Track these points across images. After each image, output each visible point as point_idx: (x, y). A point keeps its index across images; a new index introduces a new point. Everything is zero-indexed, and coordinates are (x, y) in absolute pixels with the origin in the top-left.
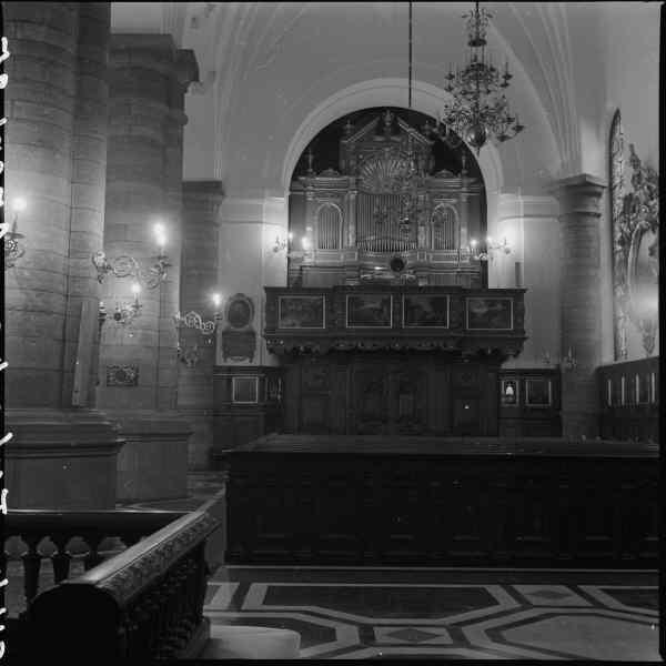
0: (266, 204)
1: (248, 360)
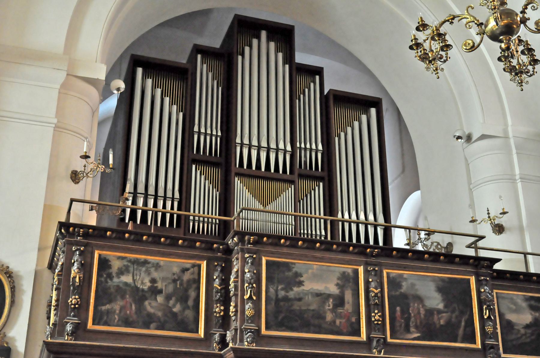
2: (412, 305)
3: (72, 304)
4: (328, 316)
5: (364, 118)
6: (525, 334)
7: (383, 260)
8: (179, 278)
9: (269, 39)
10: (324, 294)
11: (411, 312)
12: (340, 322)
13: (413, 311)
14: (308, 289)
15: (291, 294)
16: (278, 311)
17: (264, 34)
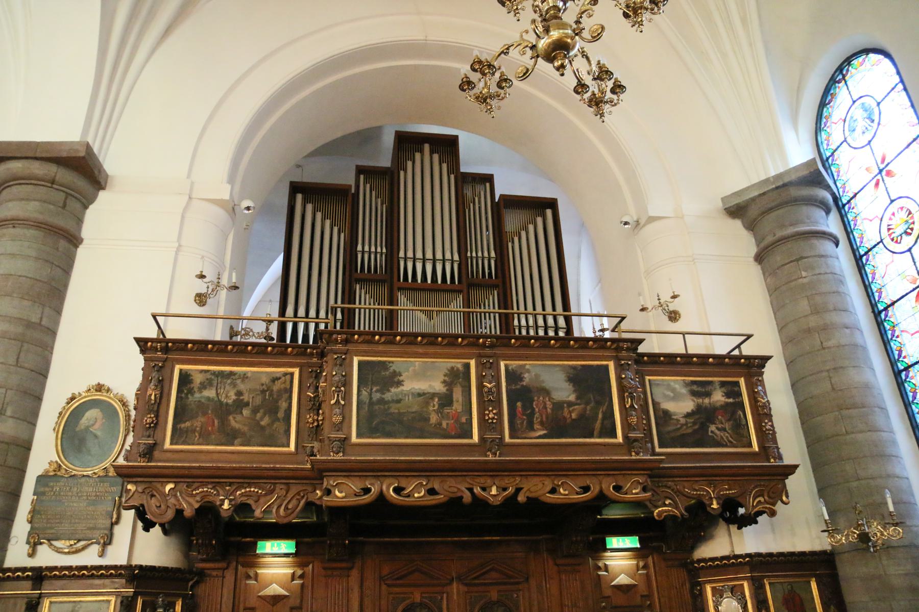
1: (95, 549)
2: (536, 398)
3: (147, 424)
4: (433, 418)
5: (539, 220)
6: (686, 424)
7: (498, 351)
8: (269, 389)
9: (432, 152)
10: (429, 393)
11: (535, 406)
12: (447, 424)
13: (537, 405)
14: (408, 389)
15: (388, 396)
16: (371, 415)
17: (427, 147)
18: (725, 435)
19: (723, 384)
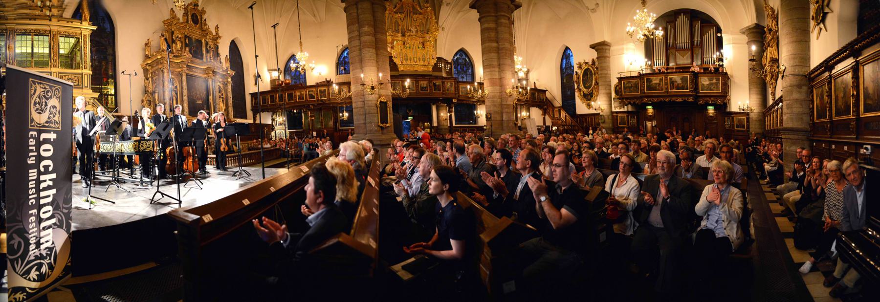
0: (625, 47)
18: (714, 89)
19: (716, 78)
